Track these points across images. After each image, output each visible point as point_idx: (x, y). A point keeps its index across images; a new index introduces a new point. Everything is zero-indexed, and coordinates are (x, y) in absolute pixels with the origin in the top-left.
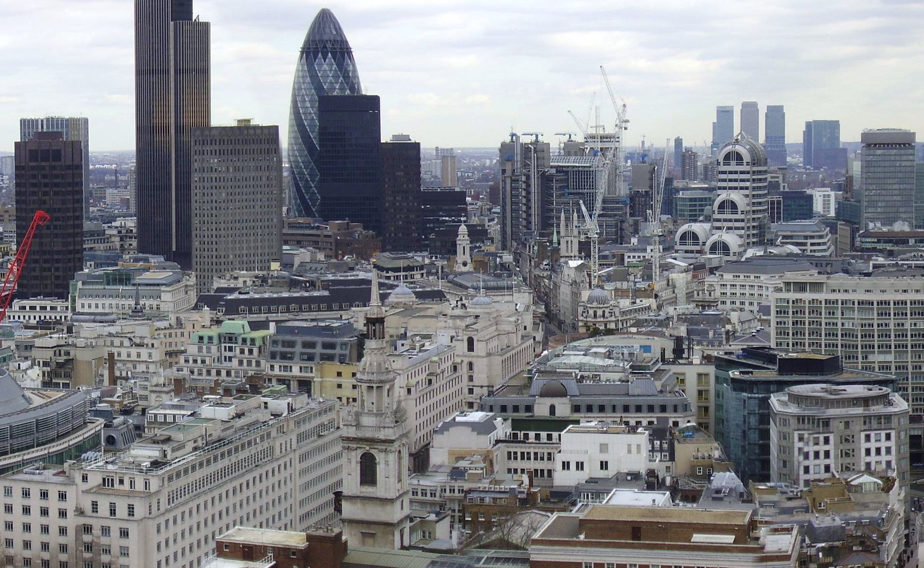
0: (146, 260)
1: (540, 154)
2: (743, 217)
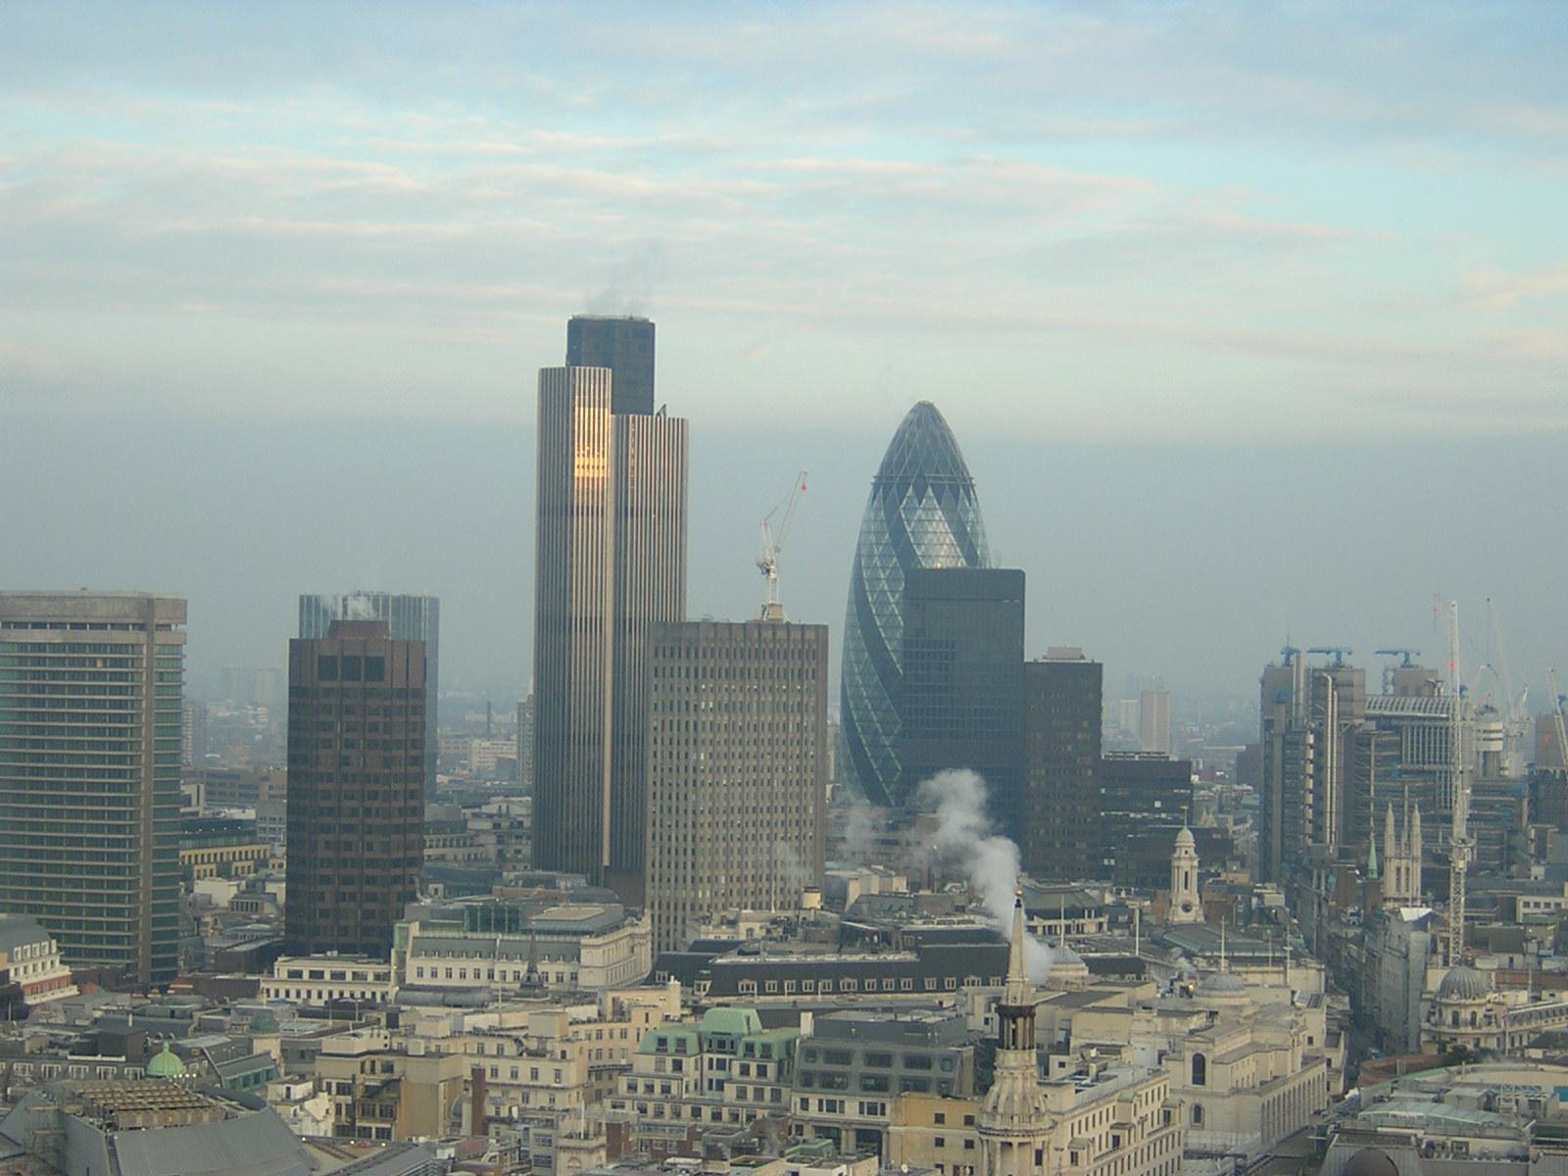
0: (550, 883)
1: (1345, 691)
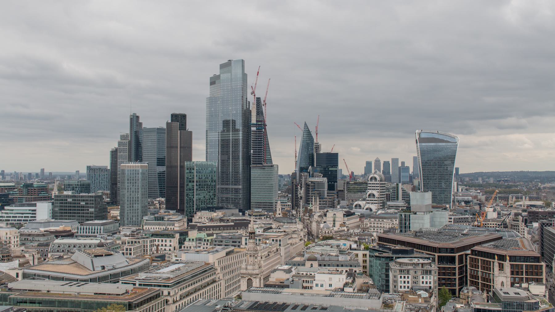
0: (169, 212)
2: (377, 199)
